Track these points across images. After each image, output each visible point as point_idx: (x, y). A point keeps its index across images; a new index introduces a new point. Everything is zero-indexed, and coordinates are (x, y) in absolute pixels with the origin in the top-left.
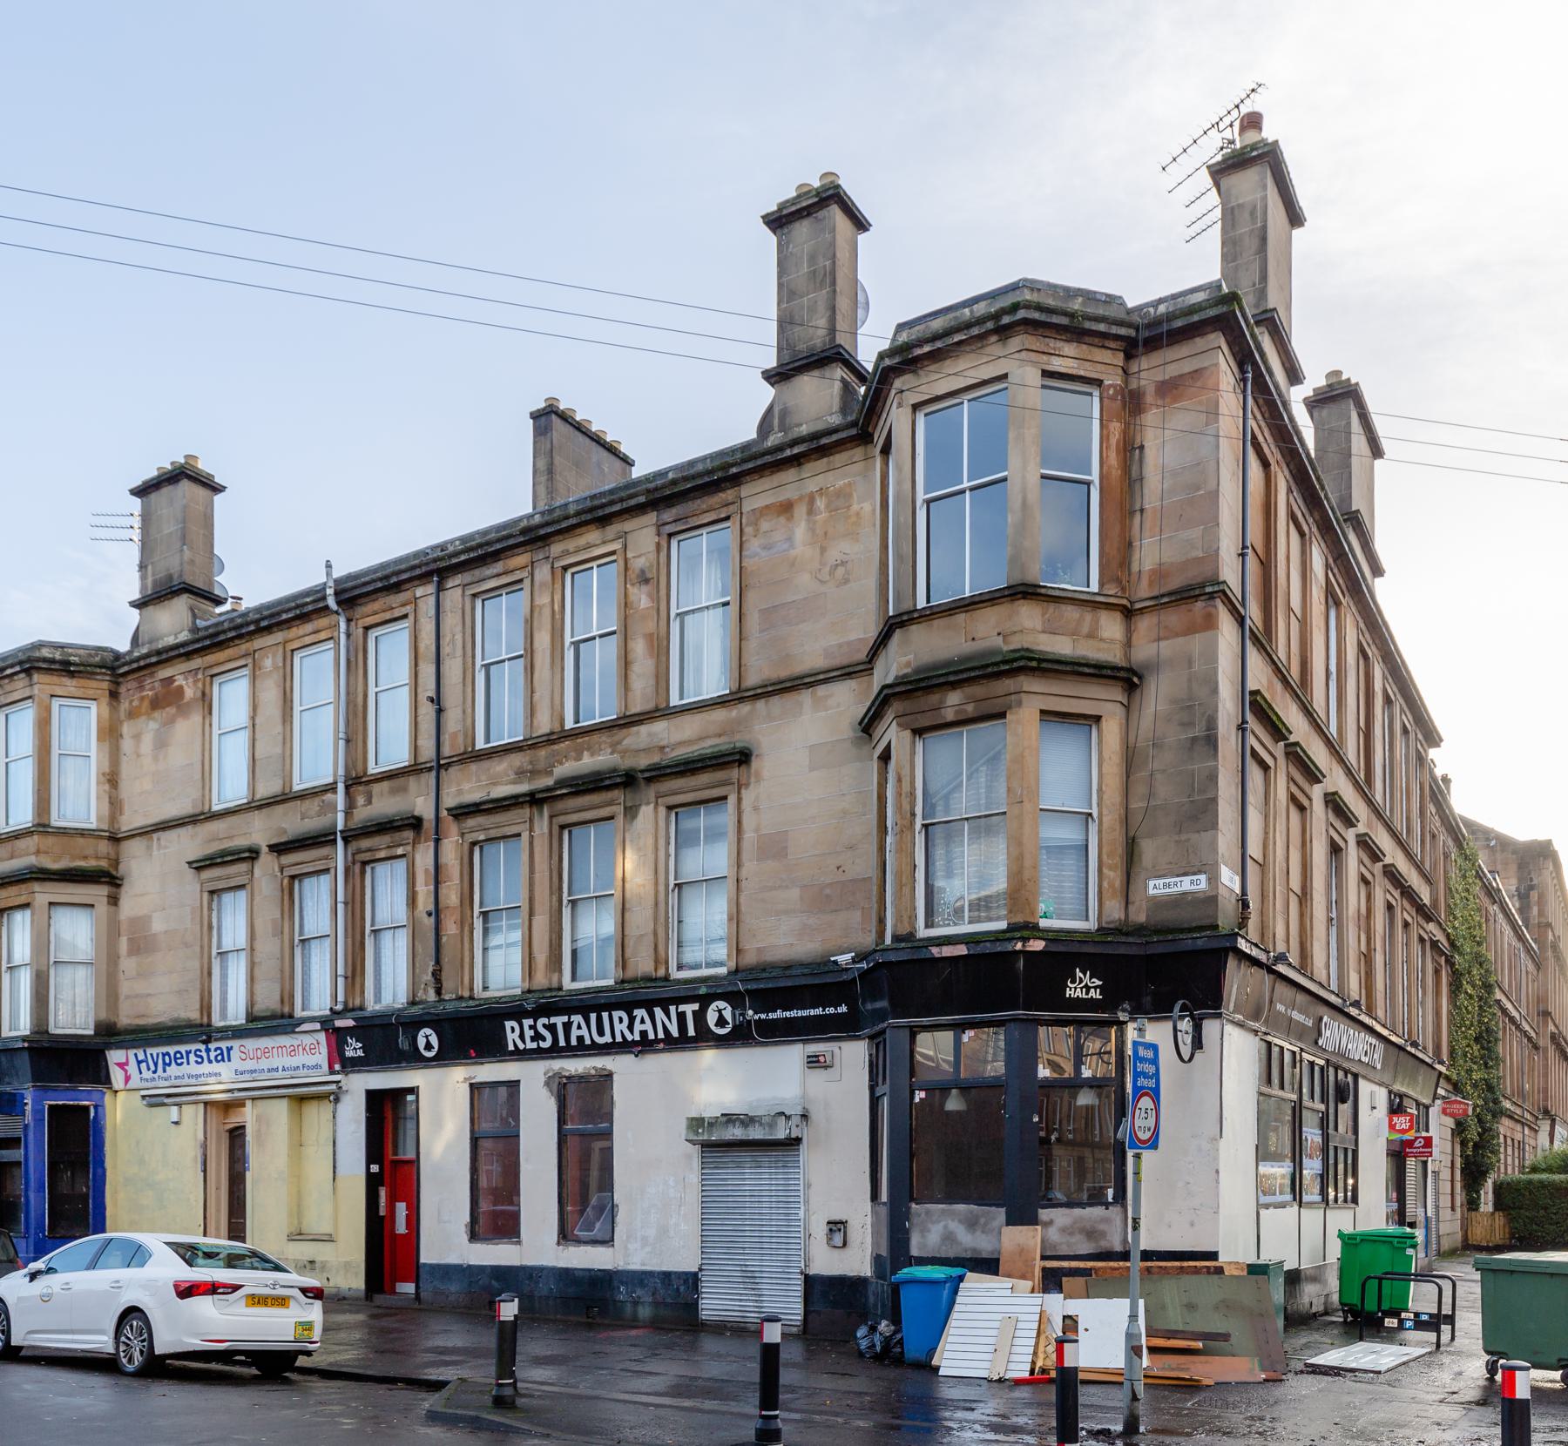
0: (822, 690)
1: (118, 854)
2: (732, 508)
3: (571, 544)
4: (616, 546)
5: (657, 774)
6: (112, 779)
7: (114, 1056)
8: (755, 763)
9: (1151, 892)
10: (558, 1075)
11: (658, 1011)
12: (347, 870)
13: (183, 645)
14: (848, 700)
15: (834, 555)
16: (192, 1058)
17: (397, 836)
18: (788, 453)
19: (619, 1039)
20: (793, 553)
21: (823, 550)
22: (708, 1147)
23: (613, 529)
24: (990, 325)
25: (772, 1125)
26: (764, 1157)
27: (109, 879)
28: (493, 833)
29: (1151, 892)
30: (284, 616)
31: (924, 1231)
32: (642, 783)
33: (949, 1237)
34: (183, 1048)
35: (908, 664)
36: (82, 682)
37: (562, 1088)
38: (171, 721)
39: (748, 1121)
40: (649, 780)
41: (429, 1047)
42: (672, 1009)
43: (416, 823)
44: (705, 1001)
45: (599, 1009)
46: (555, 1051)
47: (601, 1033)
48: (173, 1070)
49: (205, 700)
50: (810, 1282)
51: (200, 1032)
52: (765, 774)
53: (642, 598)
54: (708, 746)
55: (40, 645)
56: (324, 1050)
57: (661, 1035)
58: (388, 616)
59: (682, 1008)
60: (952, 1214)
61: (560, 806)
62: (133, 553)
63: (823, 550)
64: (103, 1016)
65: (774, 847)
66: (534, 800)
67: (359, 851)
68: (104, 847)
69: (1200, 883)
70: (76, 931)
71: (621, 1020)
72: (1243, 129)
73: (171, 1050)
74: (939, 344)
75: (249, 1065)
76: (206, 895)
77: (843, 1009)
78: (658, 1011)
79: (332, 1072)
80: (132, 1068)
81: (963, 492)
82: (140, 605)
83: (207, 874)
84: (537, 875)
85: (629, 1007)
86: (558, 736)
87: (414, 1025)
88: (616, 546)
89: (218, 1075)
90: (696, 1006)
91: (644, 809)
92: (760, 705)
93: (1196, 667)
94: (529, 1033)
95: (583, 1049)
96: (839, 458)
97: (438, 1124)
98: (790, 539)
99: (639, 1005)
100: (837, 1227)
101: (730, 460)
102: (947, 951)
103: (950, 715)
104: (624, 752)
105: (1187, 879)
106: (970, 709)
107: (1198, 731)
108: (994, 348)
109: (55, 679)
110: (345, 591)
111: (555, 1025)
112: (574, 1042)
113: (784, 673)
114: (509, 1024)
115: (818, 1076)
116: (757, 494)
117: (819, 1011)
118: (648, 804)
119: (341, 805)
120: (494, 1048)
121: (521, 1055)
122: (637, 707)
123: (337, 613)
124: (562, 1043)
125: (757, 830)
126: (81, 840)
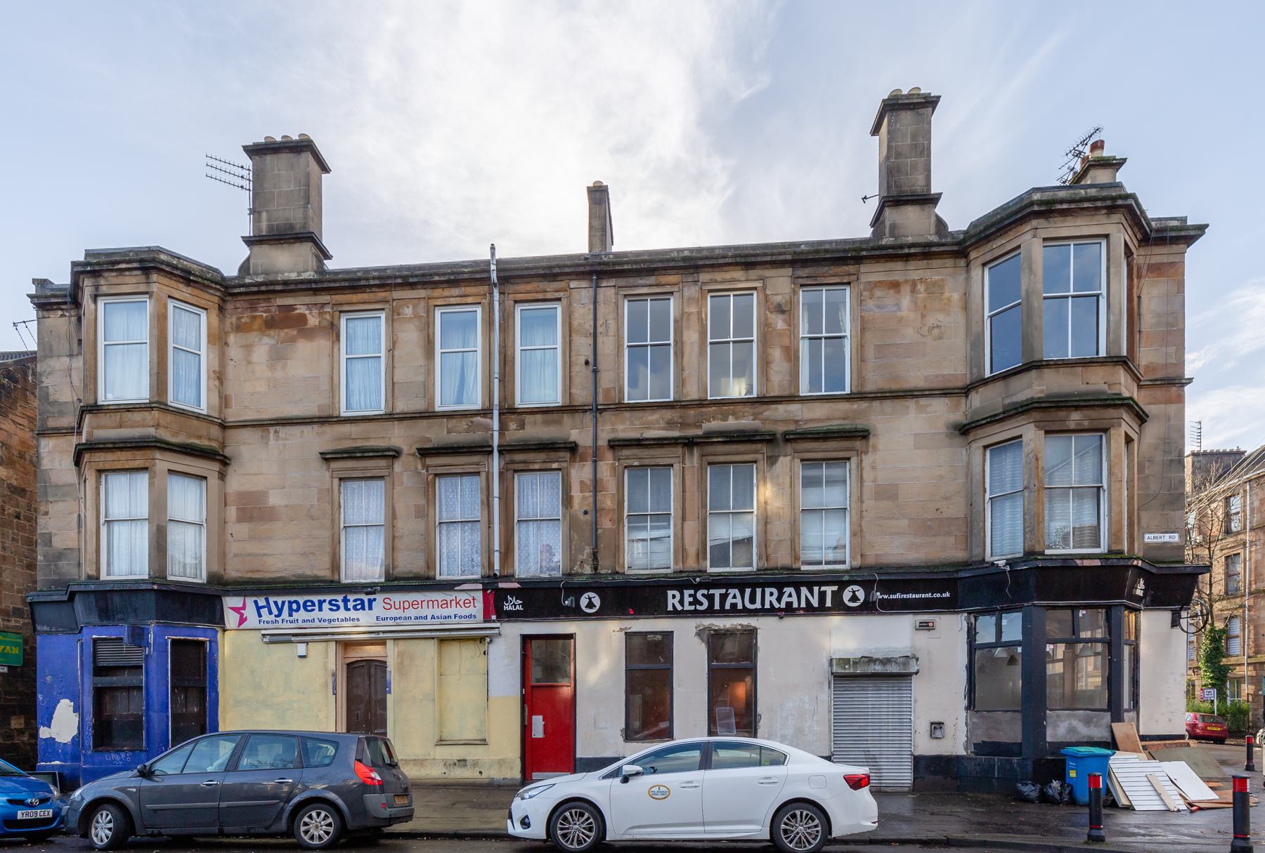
0: (923, 401)
1: (224, 439)
2: (852, 278)
3: (719, 276)
4: (758, 284)
5: (792, 438)
6: (220, 376)
7: (230, 602)
8: (872, 440)
9: (1146, 540)
10: (709, 628)
11: (804, 591)
12: (501, 474)
13: (309, 281)
14: (943, 412)
15: (931, 320)
16: (326, 606)
17: (553, 455)
18: (906, 251)
19: (767, 606)
20: (899, 314)
21: (923, 316)
22: (838, 677)
23: (754, 273)
24: (1109, 203)
25: (905, 664)
26: (883, 684)
27: (221, 458)
28: (646, 462)
29: (1146, 540)
30: (437, 278)
31: (1055, 727)
32: (781, 443)
33: (1072, 730)
34: (315, 599)
35: (1042, 391)
36: (196, 292)
37: (715, 640)
38: (293, 340)
39: (871, 660)
40: (787, 441)
41: (590, 605)
42: (816, 589)
43: (572, 448)
44: (843, 585)
45: (754, 586)
46: (710, 612)
47: (753, 601)
48: (301, 615)
49: (332, 330)
50: (917, 760)
51: (328, 586)
52: (880, 447)
53: (779, 323)
54: (835, 424)
55: (160, 250)
56: (480, 605)
57: (803, 605)
58: (540, 296)
59: (823, 588)
60: (1074, 716)
61: (710, 449)
62: (244, 200)
63: (923, 316)
64: (215, 568)
65: (887, 493)
66: (689, 443)
67: (513, 462)
68: (215, 431)
69: (1175, 538)
70: (187, 500)
71: (771, 594)
72: (1092, 150)
73: (301, 599)
74: (1073, 206)
75: (393, 613)
76: (336, 481)
77: (948, 595)
78: (804, 591)
79: (487, 619)
80: (250, 612)
81: (1067, 297)
82: (249, 242)
83: (334, 465)
84: (688, 495)
85: (780, 586)
86: (702, 403)
87: (578, 590)
88: (758, 284)
89: (357, 622)
90: (835, 588)
91: (781, 459)
92: (876, 404)
93: (1172, 422)
94: (687, 599)
95: (734, 611)
96: (935, 263)
97: (594, 659)
98: (898, 305)
99: (789, 584)
100: (936, 726)
101: (864, 246)
102: (1087, 563)
103: (1072, 426)
104: (764, 421)
105: (1167, 535)
106: (1086, 424)
107: (1174, 456)
108: (1101, 218)
109: (173, 283)
110: (504, 270)
111: (713, 595)
112: (727, 607)
113: (894, 387)
114: (670, 593)
115: (924, 635)
116: (872, 273)
117: (929, 595)
118: (786, 456)
119: (496, 426)
120: (659, 609)
121: (676, 614)
122: (775, 392)
123: (495, 285)
124: (717, 607)
125: (874, 481)
126: (195, 422)
